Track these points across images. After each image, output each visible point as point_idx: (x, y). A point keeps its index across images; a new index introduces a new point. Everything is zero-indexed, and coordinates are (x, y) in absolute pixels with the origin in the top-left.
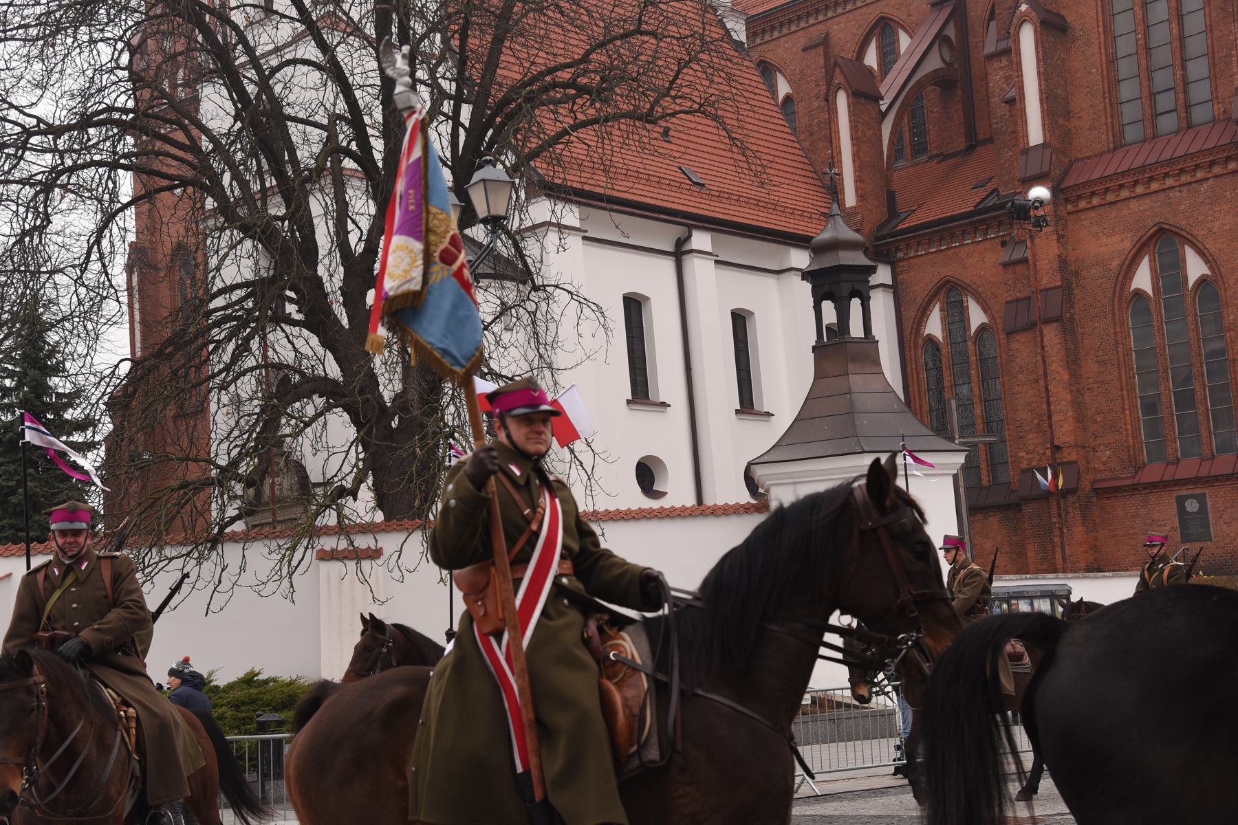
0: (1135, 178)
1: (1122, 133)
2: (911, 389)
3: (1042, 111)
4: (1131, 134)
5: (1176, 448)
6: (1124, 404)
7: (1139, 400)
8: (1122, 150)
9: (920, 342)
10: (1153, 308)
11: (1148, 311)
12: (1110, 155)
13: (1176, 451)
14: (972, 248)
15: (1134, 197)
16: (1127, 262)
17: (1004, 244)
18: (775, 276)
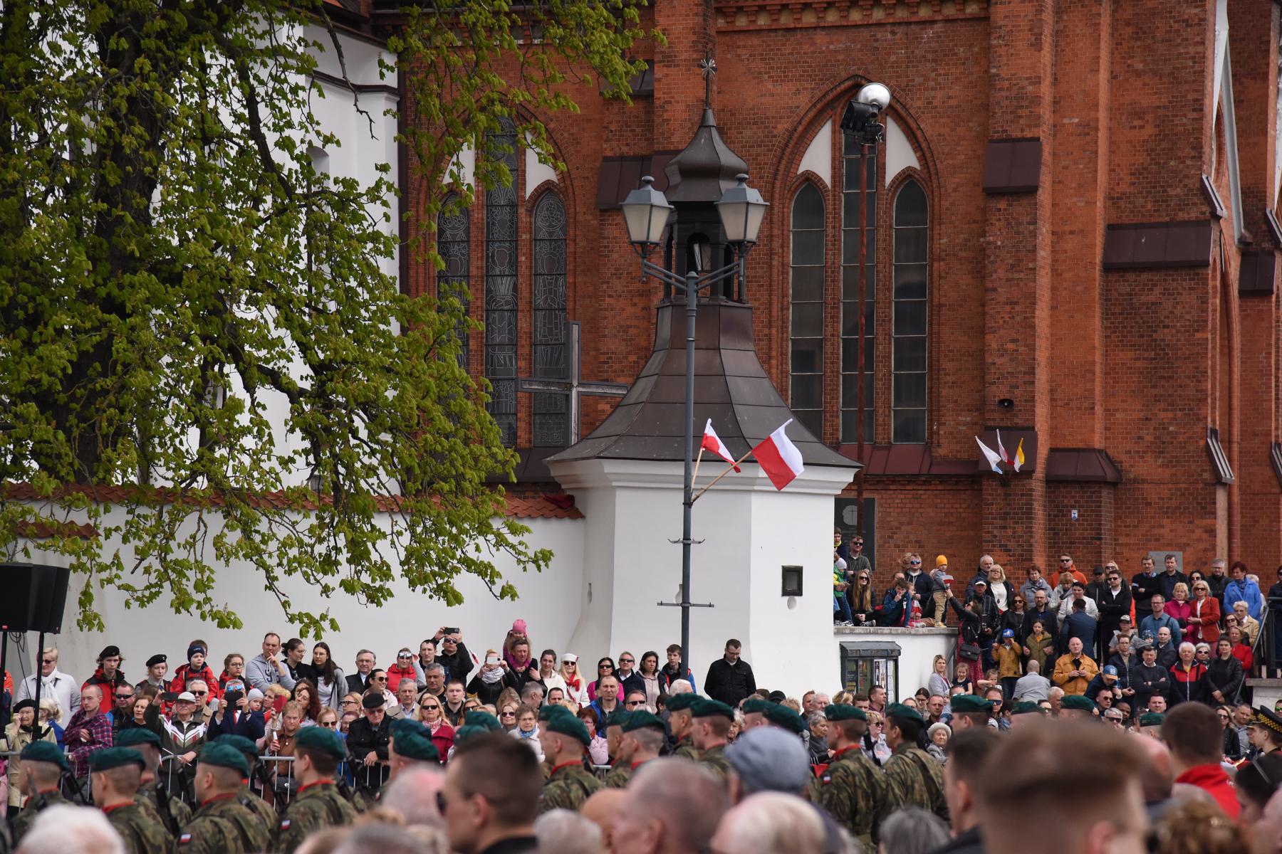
6: (770, 349)
13: (837, 430)
16: (800, 129)
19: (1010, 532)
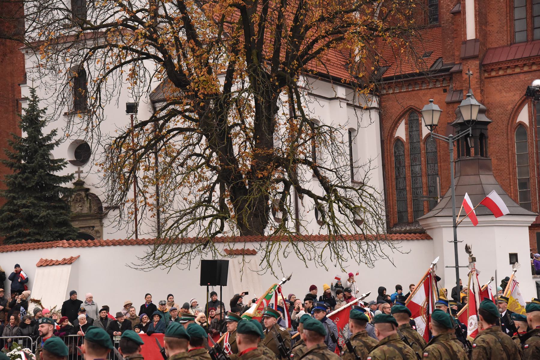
0: (525, 63)
1: (514, 35)
2: (386, 166)
3: (476, 22)
4: (520, 37)
5: (537, 207)
7: (517, 180)
8: (515, 45)
9: (393, 140)
10: (529, 132)
11: (525, 134)
12: (508, 48)
14: (426, 91)
15: (523, 73)
17: (445, 91)
18: (329, 101)
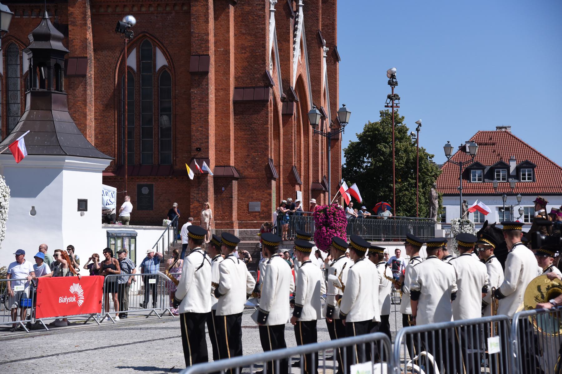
19: (200, 195)
